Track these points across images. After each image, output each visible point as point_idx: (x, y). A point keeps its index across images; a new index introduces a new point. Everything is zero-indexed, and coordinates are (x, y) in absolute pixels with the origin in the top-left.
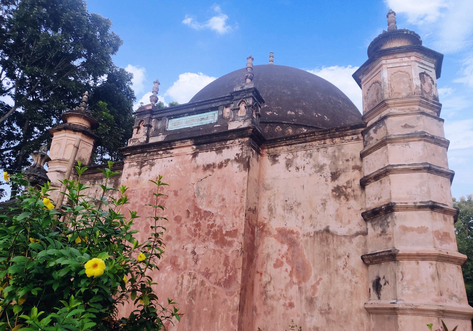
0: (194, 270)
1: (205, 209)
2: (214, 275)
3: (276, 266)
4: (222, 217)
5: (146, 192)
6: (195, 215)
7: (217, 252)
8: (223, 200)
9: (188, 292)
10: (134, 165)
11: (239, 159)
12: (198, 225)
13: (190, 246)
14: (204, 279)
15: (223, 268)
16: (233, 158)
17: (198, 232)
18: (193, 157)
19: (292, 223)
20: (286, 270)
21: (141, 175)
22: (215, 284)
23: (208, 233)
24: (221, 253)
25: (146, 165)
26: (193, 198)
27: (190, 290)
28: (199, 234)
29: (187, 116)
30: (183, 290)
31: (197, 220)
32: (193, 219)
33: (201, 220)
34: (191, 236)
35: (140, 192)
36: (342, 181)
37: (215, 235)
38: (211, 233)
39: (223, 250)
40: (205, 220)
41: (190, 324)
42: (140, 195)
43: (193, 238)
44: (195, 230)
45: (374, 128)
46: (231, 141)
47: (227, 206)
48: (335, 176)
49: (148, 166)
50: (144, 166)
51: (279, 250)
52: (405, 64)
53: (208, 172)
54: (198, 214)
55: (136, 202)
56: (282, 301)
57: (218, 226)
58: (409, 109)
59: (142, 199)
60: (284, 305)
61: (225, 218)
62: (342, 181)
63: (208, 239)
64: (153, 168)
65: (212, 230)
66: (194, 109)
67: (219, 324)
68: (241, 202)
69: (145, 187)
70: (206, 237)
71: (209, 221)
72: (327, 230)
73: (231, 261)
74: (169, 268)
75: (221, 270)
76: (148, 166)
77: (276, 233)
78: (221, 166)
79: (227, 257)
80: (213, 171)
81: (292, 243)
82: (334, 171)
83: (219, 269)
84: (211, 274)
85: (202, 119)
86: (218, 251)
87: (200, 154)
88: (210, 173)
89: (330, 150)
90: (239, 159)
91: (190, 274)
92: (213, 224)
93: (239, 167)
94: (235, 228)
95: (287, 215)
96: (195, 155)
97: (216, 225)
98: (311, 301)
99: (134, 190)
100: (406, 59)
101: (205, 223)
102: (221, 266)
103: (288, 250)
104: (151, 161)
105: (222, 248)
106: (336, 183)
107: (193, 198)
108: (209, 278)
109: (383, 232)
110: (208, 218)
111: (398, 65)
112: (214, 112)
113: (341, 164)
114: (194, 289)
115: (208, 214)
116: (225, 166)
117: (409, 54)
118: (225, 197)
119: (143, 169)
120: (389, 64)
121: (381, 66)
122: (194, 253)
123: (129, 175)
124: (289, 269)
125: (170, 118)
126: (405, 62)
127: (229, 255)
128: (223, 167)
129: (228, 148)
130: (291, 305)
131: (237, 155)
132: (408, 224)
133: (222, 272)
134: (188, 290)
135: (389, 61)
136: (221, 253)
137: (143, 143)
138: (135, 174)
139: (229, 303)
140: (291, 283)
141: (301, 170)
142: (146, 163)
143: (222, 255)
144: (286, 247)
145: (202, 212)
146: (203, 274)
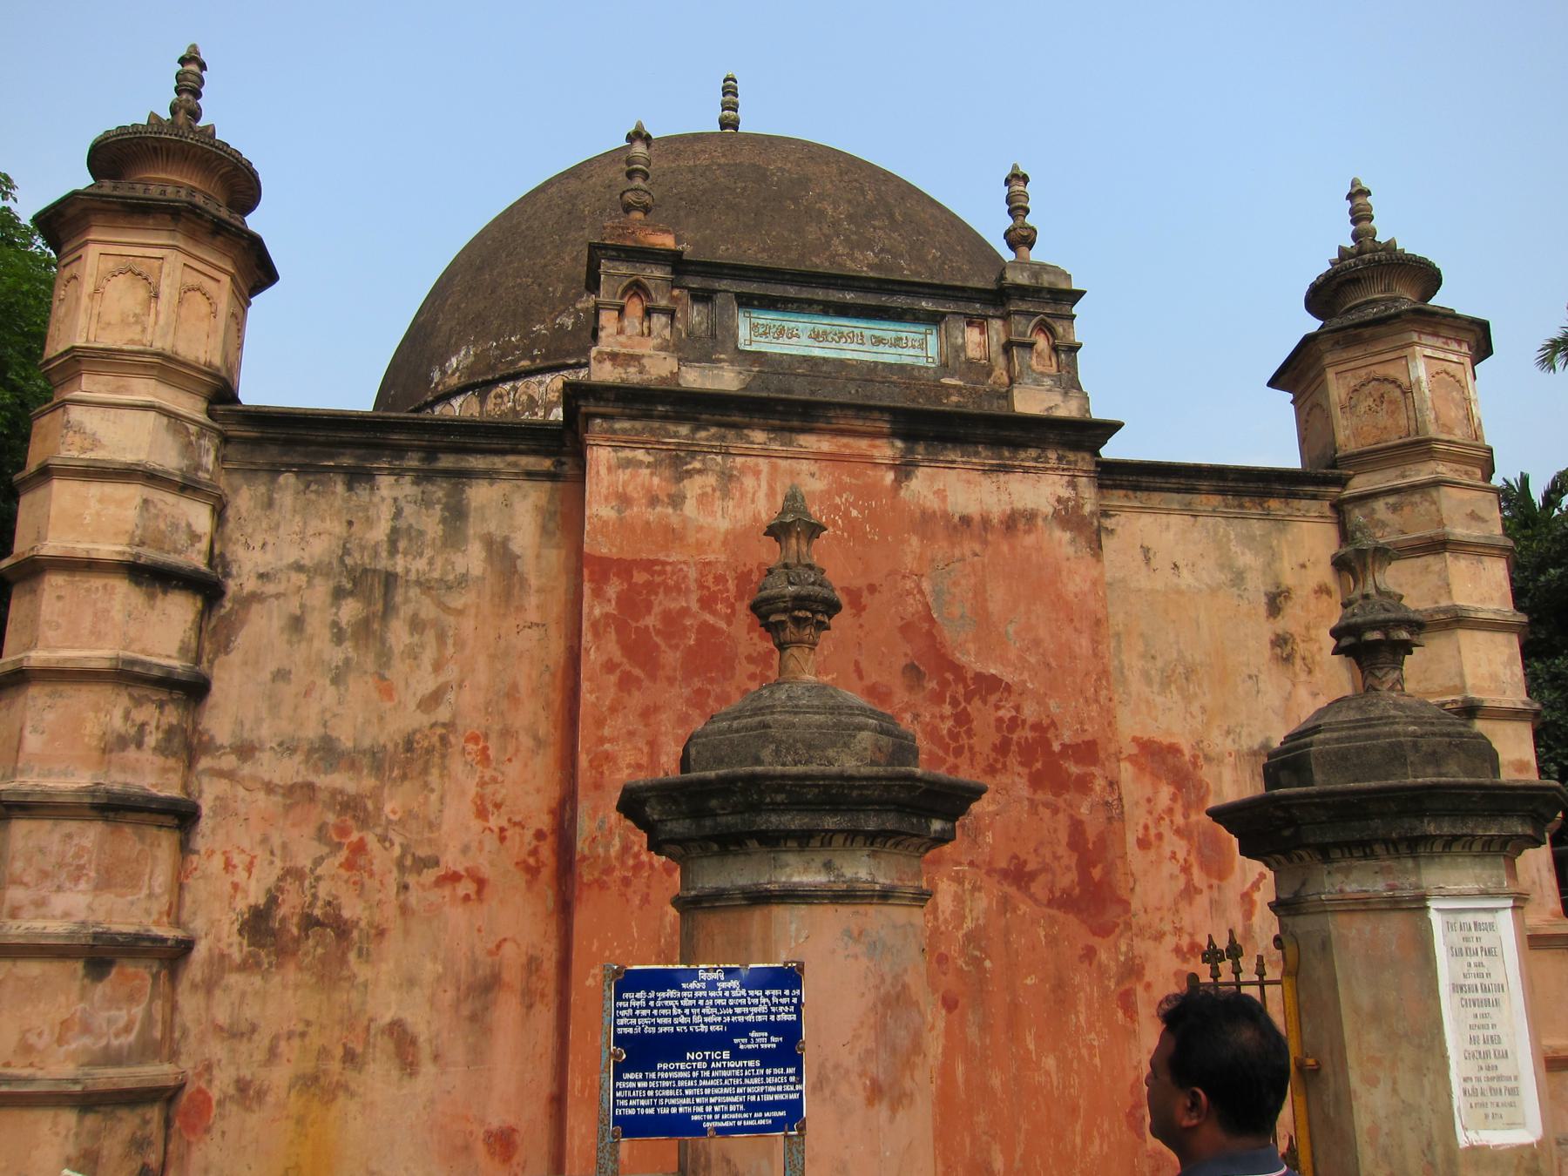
0: (971, 863)
1: (978, 667)
2: (1042, 879)
3: (1143, 844)
4: (1041, 701)
5: (720, 579)
6: (944, 684)
7: (1041, 808)
8: (1037, 642)
9: (960, 934)
10: (640, 464)
11: (1068, 516)
12: (962, 719)
14: (1012, 890)
15: (1070, 859)
16: (1051, 510)
17: (964, 740)
18: (898, 482)
20: (1173, 856)
21: (690, 508)
22: (1050, 903)
23: (1003, 748)
24: (1056, 811)
25: (700, 472)
26: (926, 626)
27: (969, 924)
28: (971, 748)
29: (817, 313)
30: (943, 928)
31: (955, 703)
32: (938, 698)
33: (968, 700)
34: (941, 753)
35: (693, 574)
36: (1290, 621)
37: (1028, 753)
38: (1014, 748)
39: (1061, 803)
40: (985, 702)
41: (985, 1028)
42: (693, 586)
43: (951, 760)
44: (954, 736)
45: (1391, 500)
46: (1033, 453)
47: (1054, 664)
49: (711, 480)
50: (690, 474)
51: (1149, 800)
52: (1454, 358)
53: (968, 547)
55: (685, 612)
56: (1170, 941)
57: (1034, 727)
58: (1466, 473)
59: (707, 603)
60: (1178, 950)
61: (1052, 704)
63: (1004, 765)
64: (733, 485)
65: (1015, 737)
66: (849, 297)
67: (1082, 1018)
68: (1095, 655)
69: (711, 557)
70: (996, 761)
71: (998, 708)
73: (1091, 833)
75: (1065, 861)
76: (711, 480)
77: (1133, 750)
79: (1077, 827)
80: (985, 543)
82: (1274, 590)
83: (1057, 858)
84: (1032, 876)
85: (879, 341)
86: (1046, 805)
87: (921, 473)
88: (977, 548)
89: (1257, 527)
90: (1068, 516)
91: (959, 879)
92: (1013, 719)
93: (1073, 541)
94: (1087, 737)
95: (1159, 699)
96: (904, 469)
97: (1024, 722)
99: (664, 563)
100: (1454, 346)
101: (984, 715)
102: (1062, 850)
103: (1174, 799)
104: (719, 458)
105: (1057, 795)
107: (926, 626)
108: (1028, 888)
110: (993, 698)
111: (1441, 355)
112: (922, 329)
114: (981, 922)
115: (989, 684)
116: (1029, 532)
117: (1462, 335)
118: (1042, 633)
119: (693, 487)
120: (1426, 346)
121: (1411, 344)
123: (624, 500)
124: (1181, 855)
125: (747, 302)
126: (1453, 352)
127: (1083, 818)
128: (1020, 534)
129: (1026, 470)
131: (1059, 500)
133: (1068, 868)
134: (958, 927)
135: (1426, 340)
136: (1056, 811)
137: (663, 380)
138: (653, 501)
139: (1103, 956)
140: (1190, 892)
141: (1185, 572)
142: (697, 465)
143: (1061, 816)
144: (1166, 792)
145: (970, 675)
146: (1005, 874)
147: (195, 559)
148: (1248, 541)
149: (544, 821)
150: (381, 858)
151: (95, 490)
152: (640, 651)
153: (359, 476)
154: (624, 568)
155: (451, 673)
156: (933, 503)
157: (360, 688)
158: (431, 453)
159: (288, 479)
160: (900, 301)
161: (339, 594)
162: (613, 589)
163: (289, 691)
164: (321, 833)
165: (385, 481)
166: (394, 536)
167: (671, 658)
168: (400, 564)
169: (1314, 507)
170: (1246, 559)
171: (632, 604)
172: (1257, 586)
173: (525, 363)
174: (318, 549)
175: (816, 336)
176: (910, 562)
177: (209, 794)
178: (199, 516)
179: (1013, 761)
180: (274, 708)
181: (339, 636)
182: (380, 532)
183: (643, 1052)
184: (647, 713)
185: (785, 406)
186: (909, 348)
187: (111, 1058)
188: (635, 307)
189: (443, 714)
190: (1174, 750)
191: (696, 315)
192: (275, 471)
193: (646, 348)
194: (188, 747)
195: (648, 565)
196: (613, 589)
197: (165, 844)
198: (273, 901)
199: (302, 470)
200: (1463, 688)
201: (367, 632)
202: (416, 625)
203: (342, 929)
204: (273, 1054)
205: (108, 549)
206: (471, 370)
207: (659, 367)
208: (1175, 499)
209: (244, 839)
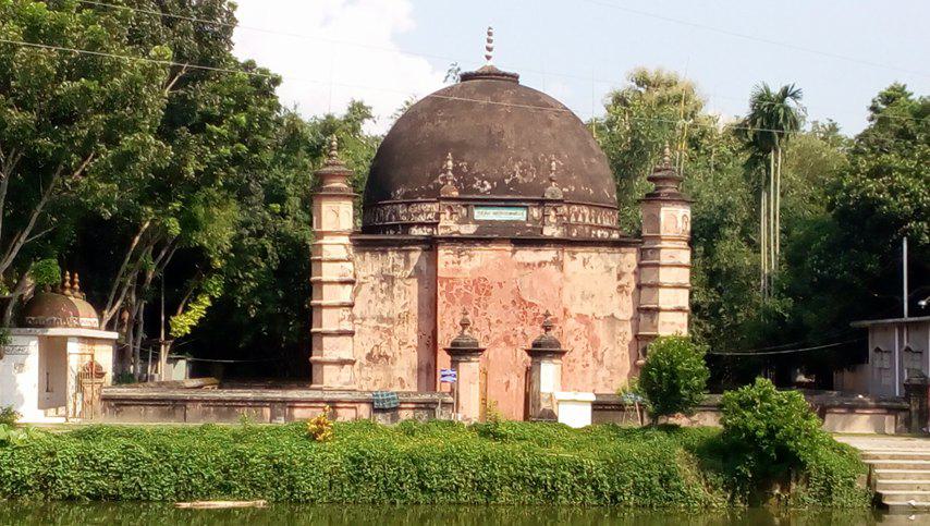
13: (520, 329)
19: (587, 309)
36: (623, 281)
48: (619, 278)
53: (529, 271)
54: (519, 301)
59: (466, 287)
62: (623, 281)
72: (613, 316)
74: (503, 344)
78: (540, 265)
81: (588, 324)
89: (617, 256)
96: (514, 252)
98: (601, 362)
106: (621, 282)
109: (652, 322)
113: (625, 269)
122: (523, 333)
125: (476, 206)
130: (587, 365)
132: (665, 320)
138: (453, 263)
144: (583, 326)
147: (351, 277)
148: (613, 259)
149: (430, 334)
150: (395, 342)
151: (332, 264)
152: (451, 299)
153: (384, 252)
154: (447, 279)
155: (408, 300)
156: (521, 260)
157: (388, 303)
158: (400, 246)
159: (368, 254)
160: (518, 204)
161: (382, 282)
162: (445, 285)
163: (372, 305)
164: (381, 337)
165: (390, 253)
166: (393, 267)
167: (458, 300)
168: (395, 273)
169: (635, 250)
170: (613, 265)
171: (449, 288)
172: (614, 273)
173: (419, 199)
174: (376, 269)
175: (495, 214)
176: (514, 276)
177: (357, 328)
178: (349, 266)
179: (536, 322)
180: (369, 308)
181: (382, 292)
182: (390, 266)
183: (443, 376)
184: (453, 313)
185: (484, 238)
186: (519, 215)
187: (346, 384)
188: (448, 213)
189: (407, 310)
190: (587, 316)
191: (464, 211)
192: (365, 251)
193: (451, 223)
194: (352, 318)
195: (452, 279)
196: (445, 285)
197: (349, 338)
198: (372, 352)
199: (370, 252)
200: (657, 304)
201: (389, 291)
202: (399, 289)
203: (387, 357)
204: (375, 384)
205: (336, 279)
206: (404, 197)
207: (455, 228)
208: (593, 249)
209: (364, 339)
